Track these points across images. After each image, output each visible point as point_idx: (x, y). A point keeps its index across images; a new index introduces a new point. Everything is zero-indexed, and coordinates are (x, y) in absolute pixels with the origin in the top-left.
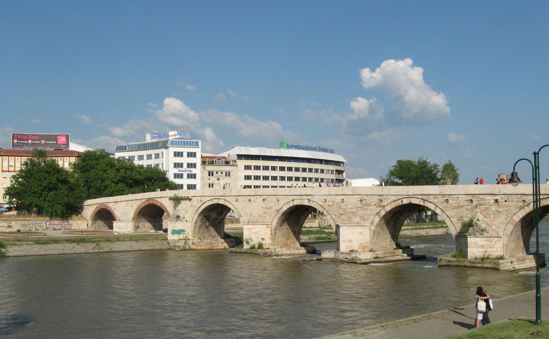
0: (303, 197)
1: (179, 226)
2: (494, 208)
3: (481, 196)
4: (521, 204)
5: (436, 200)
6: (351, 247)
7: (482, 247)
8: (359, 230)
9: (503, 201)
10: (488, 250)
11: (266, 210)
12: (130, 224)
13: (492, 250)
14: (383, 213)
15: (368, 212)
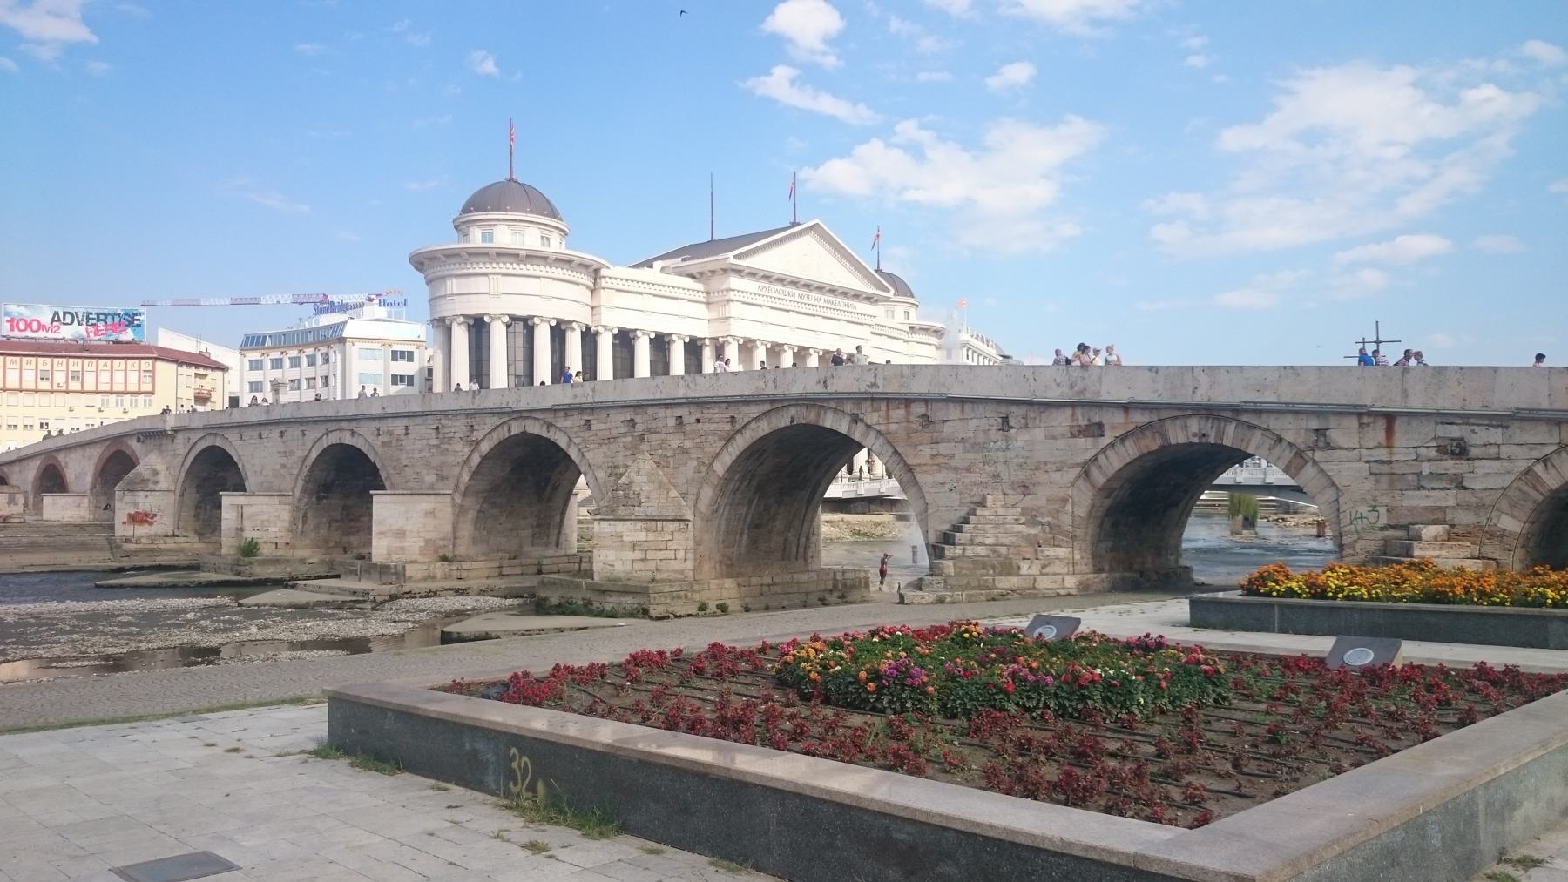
0: (345, 425)
1: (145, 502)
2: (675, 441)
3: (650, 410)
4: (728, 427)
5: (568, 423)
6: (403, 548)
7: (634, 546)
8: (426, 504)
9: (693, 419)
10: (650, 555)
11: (284, 461)
12: (86, 500)
13: (661, 555)
14: (476, 460)
15: (450, 459)
